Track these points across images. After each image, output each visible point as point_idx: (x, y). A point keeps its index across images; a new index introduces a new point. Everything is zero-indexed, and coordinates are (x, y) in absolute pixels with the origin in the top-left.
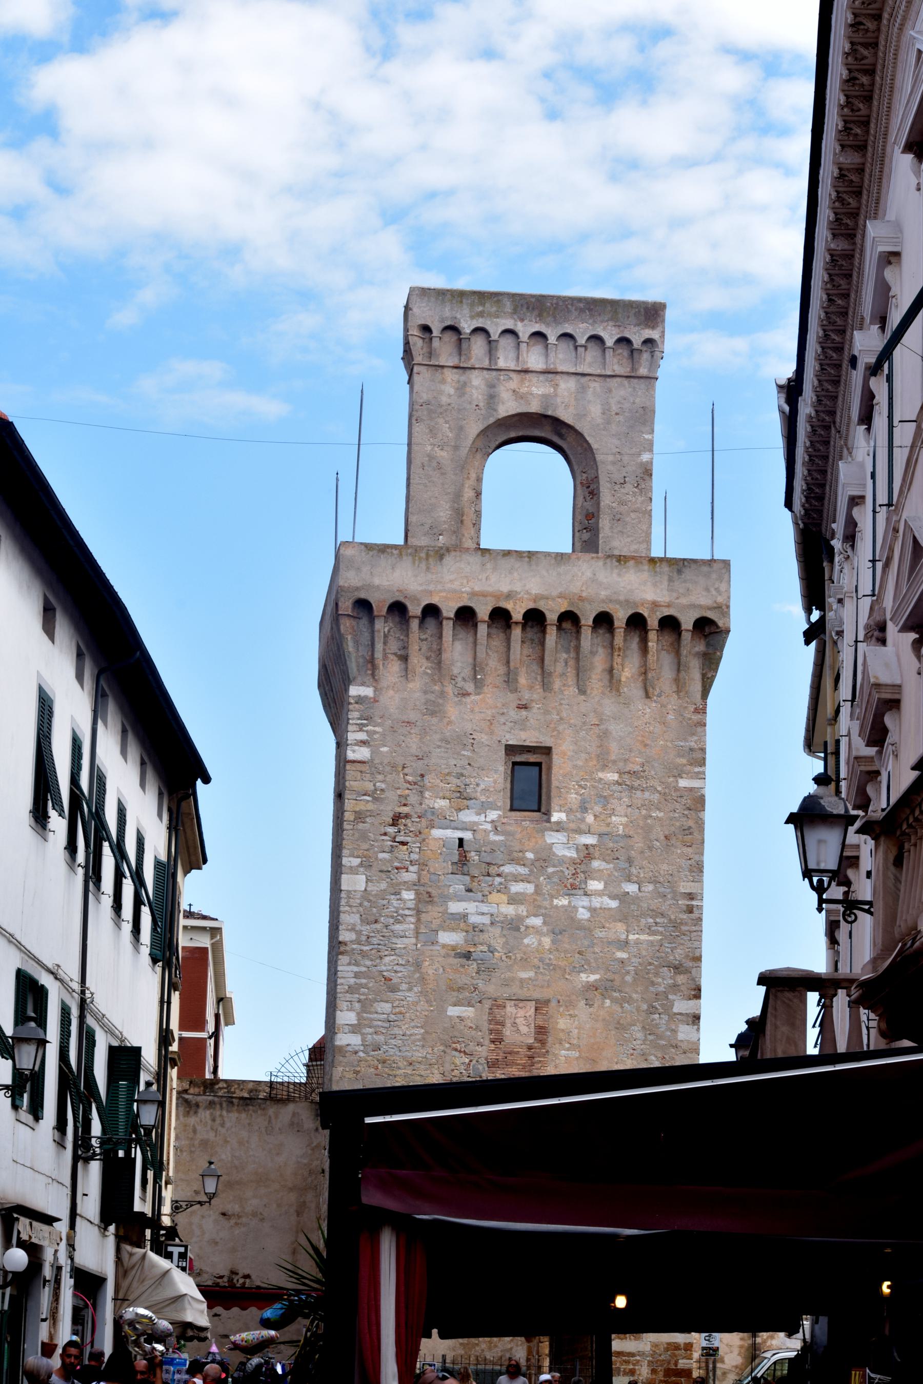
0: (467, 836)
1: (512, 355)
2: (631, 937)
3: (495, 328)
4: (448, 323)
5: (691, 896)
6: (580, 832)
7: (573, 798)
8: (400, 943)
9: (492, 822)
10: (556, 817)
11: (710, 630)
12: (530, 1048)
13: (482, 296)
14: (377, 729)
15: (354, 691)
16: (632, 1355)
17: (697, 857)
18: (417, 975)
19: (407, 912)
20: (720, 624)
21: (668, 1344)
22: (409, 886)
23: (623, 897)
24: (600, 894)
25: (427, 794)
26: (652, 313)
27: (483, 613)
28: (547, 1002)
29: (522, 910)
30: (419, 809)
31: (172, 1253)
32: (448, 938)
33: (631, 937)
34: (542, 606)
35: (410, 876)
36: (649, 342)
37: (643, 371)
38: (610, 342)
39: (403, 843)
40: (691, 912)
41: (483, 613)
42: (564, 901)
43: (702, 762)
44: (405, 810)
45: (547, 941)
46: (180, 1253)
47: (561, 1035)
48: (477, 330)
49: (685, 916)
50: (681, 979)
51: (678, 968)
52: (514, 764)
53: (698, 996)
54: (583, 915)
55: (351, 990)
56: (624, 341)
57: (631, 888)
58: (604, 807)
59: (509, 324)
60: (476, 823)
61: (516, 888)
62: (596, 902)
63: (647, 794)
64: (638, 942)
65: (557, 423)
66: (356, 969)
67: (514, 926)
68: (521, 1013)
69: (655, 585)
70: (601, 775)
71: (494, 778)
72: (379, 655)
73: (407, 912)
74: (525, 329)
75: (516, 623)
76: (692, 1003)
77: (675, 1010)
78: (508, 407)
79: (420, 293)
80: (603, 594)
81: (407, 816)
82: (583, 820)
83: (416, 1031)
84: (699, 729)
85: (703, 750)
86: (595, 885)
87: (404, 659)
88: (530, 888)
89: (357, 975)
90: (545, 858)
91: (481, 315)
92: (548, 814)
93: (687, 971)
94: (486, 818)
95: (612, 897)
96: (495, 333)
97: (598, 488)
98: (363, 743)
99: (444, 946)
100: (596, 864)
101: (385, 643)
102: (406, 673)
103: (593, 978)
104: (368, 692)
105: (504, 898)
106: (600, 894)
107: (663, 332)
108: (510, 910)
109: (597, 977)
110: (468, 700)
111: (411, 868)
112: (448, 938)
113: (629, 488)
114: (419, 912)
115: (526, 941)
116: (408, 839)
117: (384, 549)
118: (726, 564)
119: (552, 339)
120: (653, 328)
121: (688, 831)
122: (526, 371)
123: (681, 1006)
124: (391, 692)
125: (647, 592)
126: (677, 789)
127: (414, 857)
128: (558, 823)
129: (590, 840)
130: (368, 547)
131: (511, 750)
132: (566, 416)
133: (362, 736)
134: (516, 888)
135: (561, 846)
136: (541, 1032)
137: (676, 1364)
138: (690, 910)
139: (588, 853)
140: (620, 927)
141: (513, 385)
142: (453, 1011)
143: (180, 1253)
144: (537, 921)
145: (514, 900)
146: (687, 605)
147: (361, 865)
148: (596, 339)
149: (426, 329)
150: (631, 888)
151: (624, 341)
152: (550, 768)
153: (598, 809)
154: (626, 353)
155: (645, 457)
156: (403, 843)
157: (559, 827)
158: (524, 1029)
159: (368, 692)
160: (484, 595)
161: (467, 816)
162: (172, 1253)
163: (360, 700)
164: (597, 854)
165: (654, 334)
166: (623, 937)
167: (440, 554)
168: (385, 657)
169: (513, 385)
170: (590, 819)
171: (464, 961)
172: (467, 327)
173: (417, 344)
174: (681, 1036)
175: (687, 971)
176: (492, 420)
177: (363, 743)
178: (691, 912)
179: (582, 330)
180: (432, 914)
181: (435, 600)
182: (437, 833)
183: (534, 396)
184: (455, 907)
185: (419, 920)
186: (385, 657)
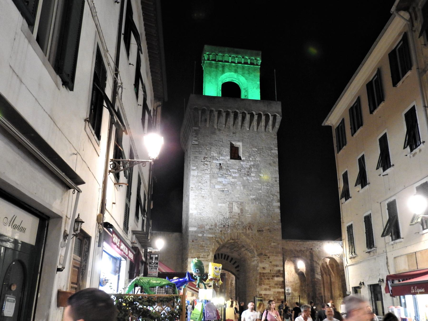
0: (221, 162)
12: (239, 214)
16: (269, 295)
28: (243, 203)
29: (236, 180)
31: (152, 257)
32: (217, 187)
39: (206, 164)
44: (206, 156)
55: (194, 199)
66: (194, 194)
69: (264, 106)
70: (253, 149)
72: (200, 119)
88: (237, 175)
89: (195, 196)
103: (254, 197)
105: (231, 177)
108: (233, 180)
134: (234, 175)
136: (242, 210)
145: (234, 178)
162: (152, 257)
168: (201, 121)
170: (251, 159)
171: (222, 193)
182: (214, 161)
185: (211, 182)
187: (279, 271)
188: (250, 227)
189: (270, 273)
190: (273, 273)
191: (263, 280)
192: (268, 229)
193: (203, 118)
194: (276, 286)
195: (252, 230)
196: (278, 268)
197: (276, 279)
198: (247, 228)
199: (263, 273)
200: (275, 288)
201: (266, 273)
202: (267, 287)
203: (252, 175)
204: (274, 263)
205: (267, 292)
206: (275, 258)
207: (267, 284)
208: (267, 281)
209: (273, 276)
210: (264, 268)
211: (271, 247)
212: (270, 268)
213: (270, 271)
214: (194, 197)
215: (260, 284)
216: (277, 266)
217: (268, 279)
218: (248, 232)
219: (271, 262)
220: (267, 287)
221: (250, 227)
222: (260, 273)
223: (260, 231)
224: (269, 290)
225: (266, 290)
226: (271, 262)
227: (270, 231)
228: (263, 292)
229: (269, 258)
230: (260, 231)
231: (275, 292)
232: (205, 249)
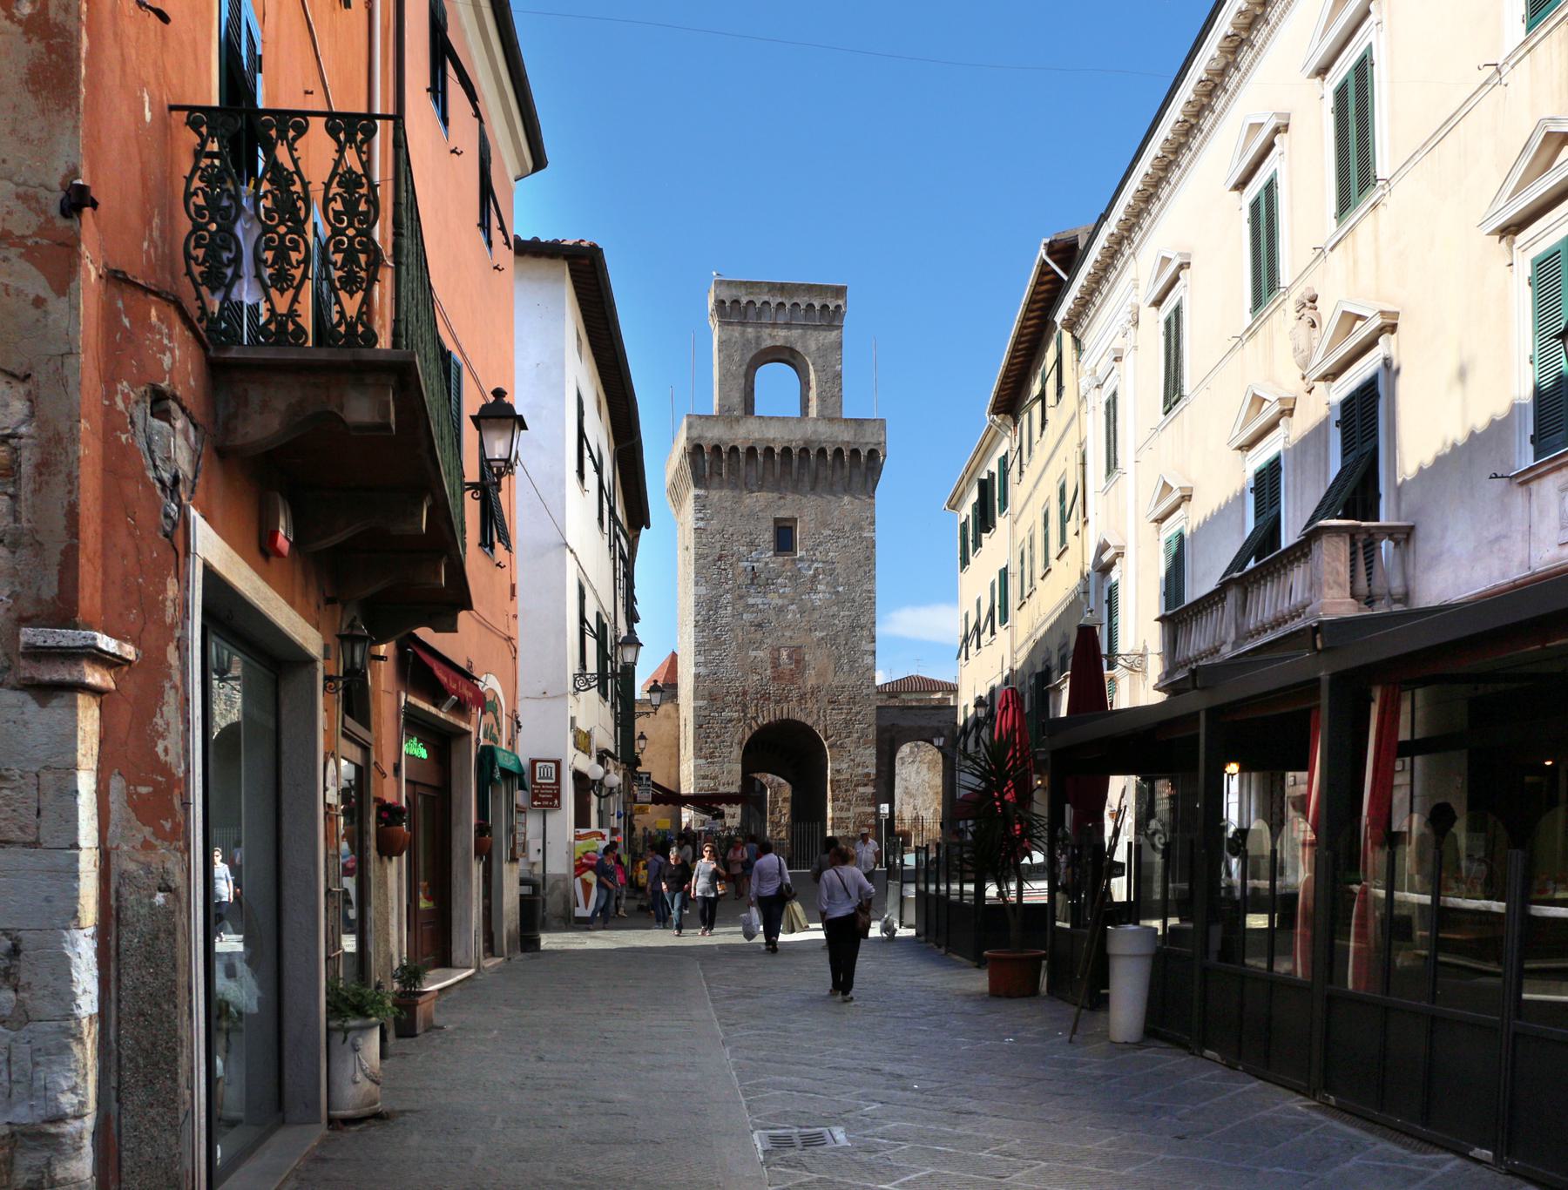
26: (840, 292)
38: (817, 307)
43: (873, 523)
48: (751, 302)
59: (766, 298)
65: (792, 351)
67: (781, 610)
71: (767, 537)
74: (774, 301)
78: (768, 343)
79: (719, 283)
86: (821, 587)
94: (767, 557)
108: (780, 602)
117: (708, 418)
118: (883, 420)
125: (845, 436)
130: (700, 417)
132: (799, 348)
142: (753, 654)
145: (780, 596)
151: (825, 307)
165: (840, 302)
167: (738, 420)
172: (744, 300)
179: (803, 301)
183: (781, 337)
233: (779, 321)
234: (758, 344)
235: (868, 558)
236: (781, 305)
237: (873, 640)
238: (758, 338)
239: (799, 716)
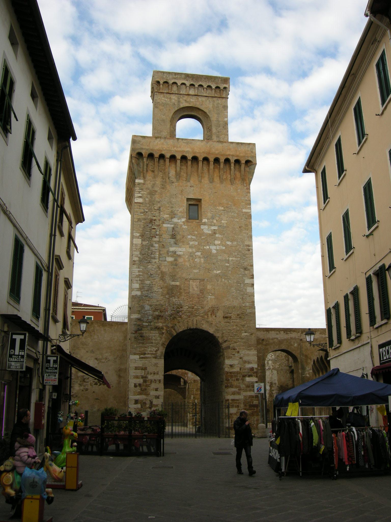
1: (185, 90)
2: (230, 259)
3: (179, 83)
4: (165, 80)
5: (249, 246)
6: (211, 225)
7: (209, 215)
8: (154, 261)
9: (183, 222)
10: (204, 220)
11: (250, 163)
13: (176, 74)
14: (145, 193)
15: (137, 181)
17: (250, 233)
18: (159, 272)
19: (156, 251)
20: (253, 162)
21: (250, 396)
22: (156, 242)
23: (226, 246)
24: (219, 245)
25: (161, 213)
27: (179, 157)
29: (194, 250)
30: (159, 218)
31: (50, 360)
33: (230, 259)
34: (197, 155)
35: (156, 239)
36: (225, 88)
37: (224, 96)
38: (214, 87)
39: (154, 229)
40: (249, 251)
41: (179, 157)
42: (208, 247)
43: (250, 204)
44: (154, 218)
45: (202, 260)
46: (54, 360)
47: (209, 291)
49: (247, 252)
50: (246, 272)
51: (245, 269)
52: (190, 205)
53: (253, 278)
54: (214, 251)
56: (217, 87)
57: (229, 243)
58: (219, 218)
60: (178, 222)
61: (191, 243)
62: (218, 248)
63: (233, 214)
64: (232, 260)
66: (138, 269)
68: (195, 284)
73: (156, 251)
74: (188, 84)
75: (189, 160)
76: (251, 280)
77: (246, 282)
78: (184, 104)
80: (217, 152)
81: (155, 220)
82: (213, 222)
83: (160, 290)
84: (248, 194)
85: (250, 201)
87: (153, 171)
88: (197, 243)
90: (201, 234)
91: (175, 78)
92: (201, 220)
93: (249, 270)
94: (181, 221)
95: (223, 245)
96: (179, 84)
97: (212, 128)
98: (140, 197)
99: (168, 262)
100: (217, 235)
101: (147, 167)
102: (155, 177)
103: (218, 272)
104: (141, 181)
106: (219, 245)
107: (229, 85)
108: (190, 250)
109: (220, 272)
110: (174, 184)
111: (157, 237)
112: (170, 259)
113: (221, 127)
114: (160, 251)
115: (196, 260)
116: (155, 227)
119: (196, 86)
120: (226, 84)
121: (246, 225)
122: (189, 95)
123: (247, 281)
124: (149, 182)
126: (242, 212)
127: (158, 233)
128: (204, 222)
129: (216, 228)
130: (142, 137)
131: (188, 200)
133: (140, 195)
135: (206, 229)
137: (253, 403)
138: (249, 250)
139: (214, 232)
140: (226, 256)
141: (185, 99)
143: (54, 360)
144: (199, 254)
145: (191, 247)
146: (242, 155)
147: (140, 236)
148: (209, 87)
149: (158, 82)
150: (229, 243)
151: (217, 87)
152: (201, 206)
153: (217, 218)
154: (218, 91)
155: (226, 119)
156: (154, 229)
157: (205, 224)
158: (196, 289)
159: (141, 181)
160: (179, 151)
161: (175, 220)
162: (50, 360)
163: (139, 184)
164: (218, 232)
166: (228, 259)
169: (185, 99)
170: (215, 221)
172: (171, 82)
173: (155, 86)
174: (248, 291)
175: (249, 270)
176: (179, 108)
177: (140, 197)
178: (249, 251)
180: (164, 251)
181: (163, 153)
182: (165, 225)
184: (172, 249)
186: (147, 171)
187: (252, 369)
188: (213, 312)
189: (240, 373)
190: (244, 372)
191: (230, 381)
192: (238, 315)
193: (150, 168)
194: (248, 389)
195: (216, 316)
196: (250, 366)
197: (248, 379)
198: (209, 313)
199: (231, 373)
200: (246, 391)
201: (234, 373)
202: (236, 390)
203: (217, 242)
204: (246, 358)
205: (236, 397)
206: (247, 352)
207: (236, 387)
208: (235, 383)
209: (244, 376)
210: (231, 366)
211: (242, 339)
212: (240, 366)
213: (240, 369)
214: (137, 274)
215: (227, 387)
216: (249, 362)
217: (237, 380)
218: (210, 319)
219: (241, 358)
220: (236, 390)
221: (213, 312)
222: (227, 373)
223: (226, 317)
224: (239, 393)
225: (234, 393)
226: (241, 358)
227: (240, 318)
228: (230, 397)
229: (238, 352)
230: (226, 317)
231: (244, 396)
232: (152, 343)
233: (192, 95)
234: (179, 105)
235: (246, 225)
236: (192, 85)
237: (252, 277)
238: (179, 102)
239: (205, 327)
